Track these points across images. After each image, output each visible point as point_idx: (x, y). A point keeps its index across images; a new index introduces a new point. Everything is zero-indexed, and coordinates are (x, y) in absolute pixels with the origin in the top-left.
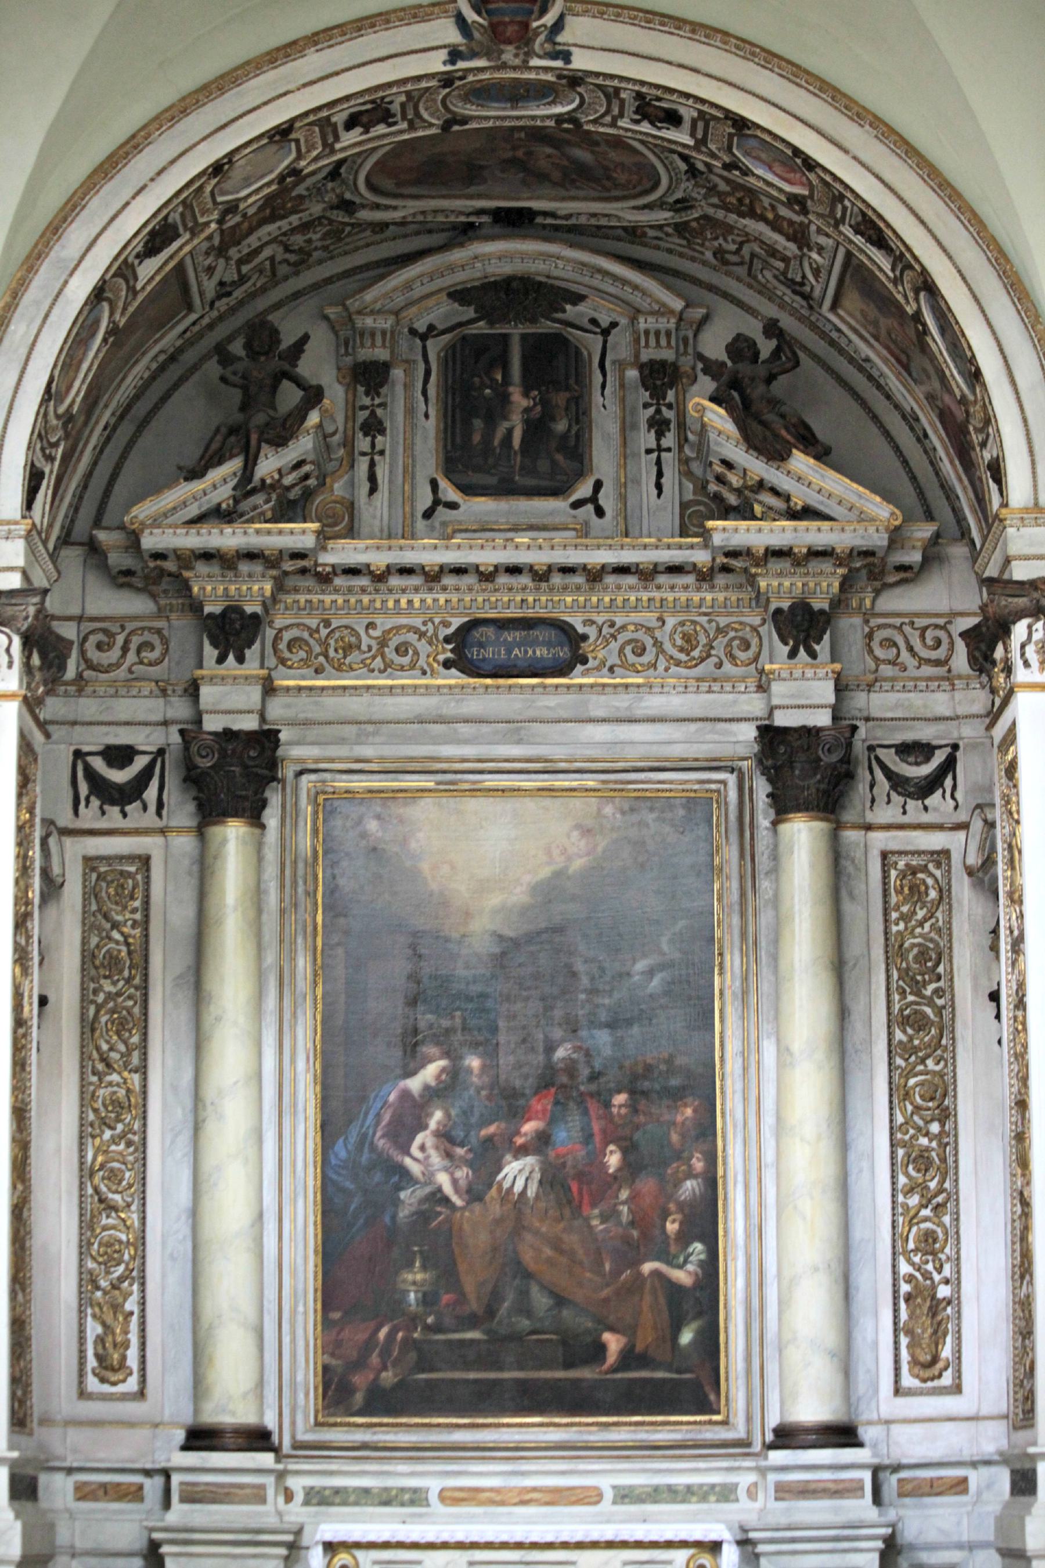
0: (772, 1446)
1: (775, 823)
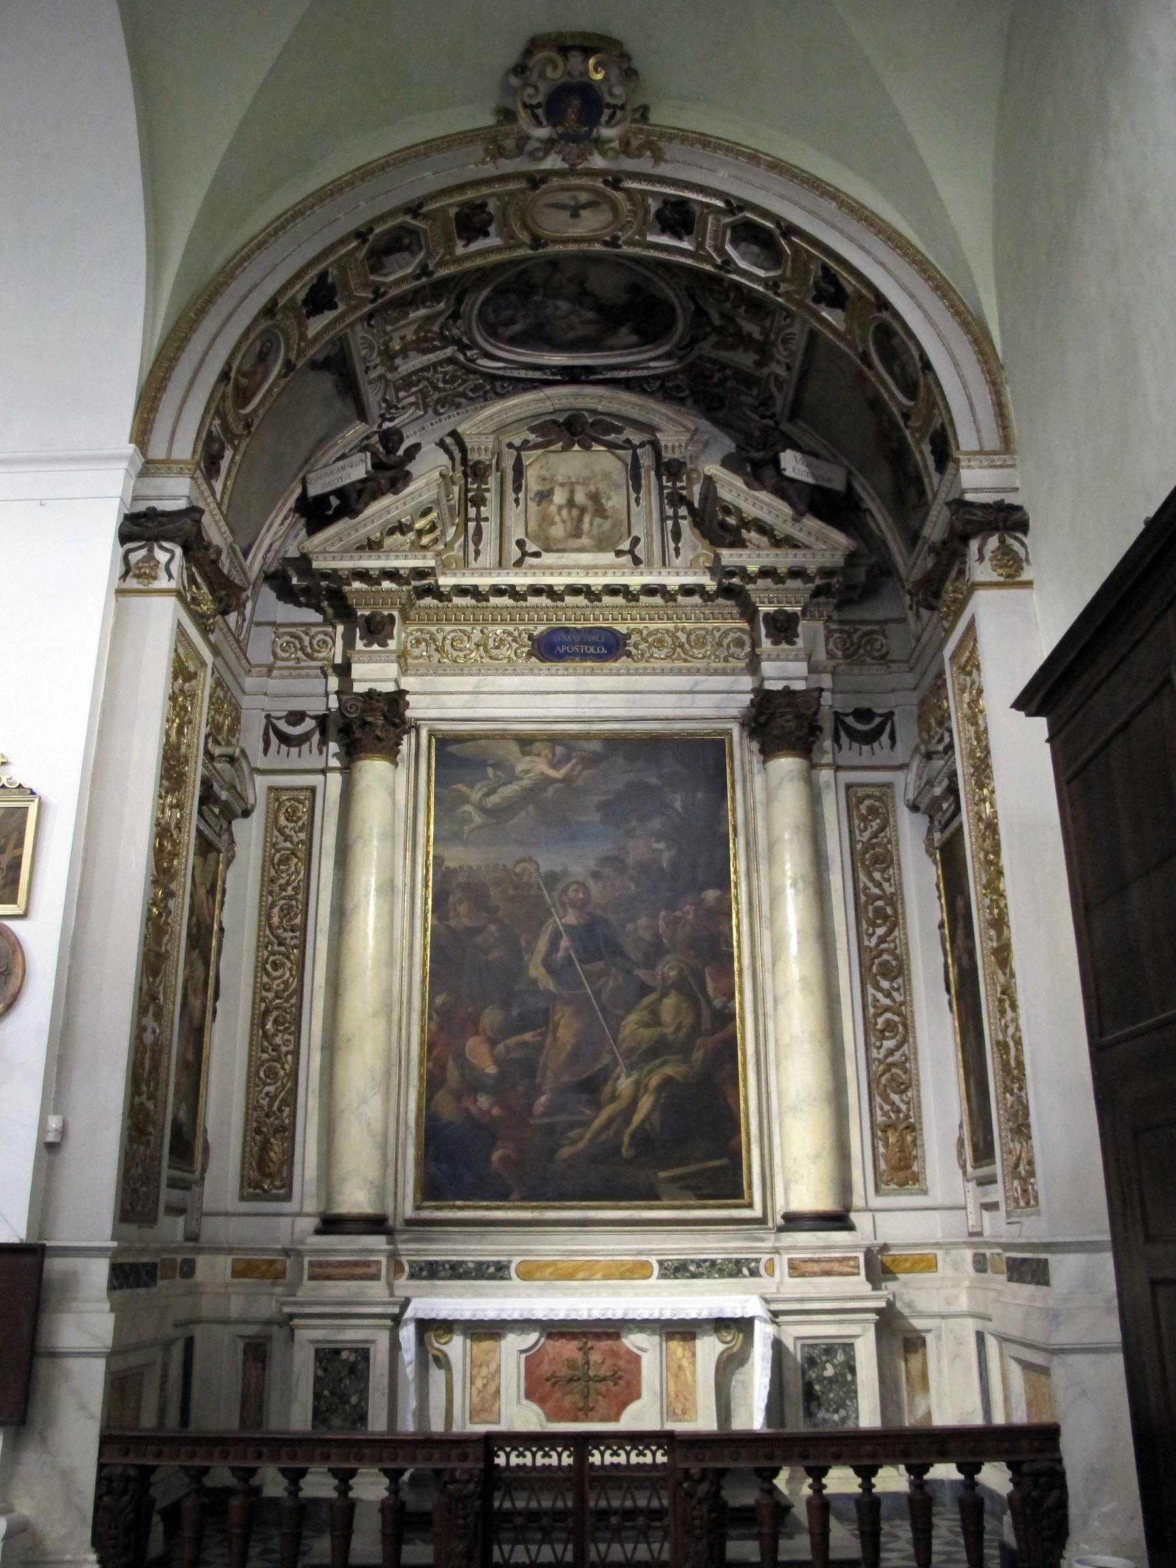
0: (781, 1229)
1: (764, 762)
